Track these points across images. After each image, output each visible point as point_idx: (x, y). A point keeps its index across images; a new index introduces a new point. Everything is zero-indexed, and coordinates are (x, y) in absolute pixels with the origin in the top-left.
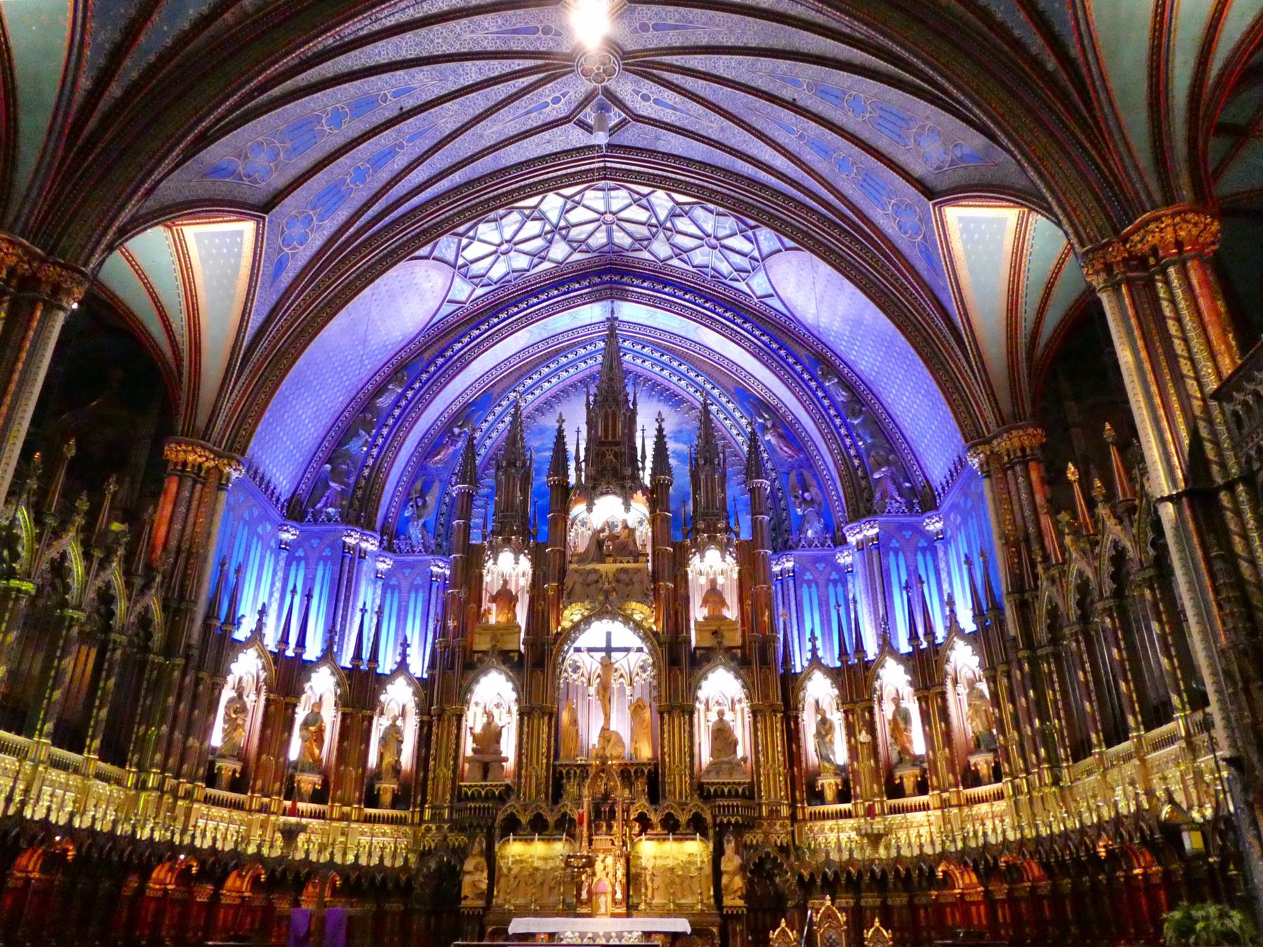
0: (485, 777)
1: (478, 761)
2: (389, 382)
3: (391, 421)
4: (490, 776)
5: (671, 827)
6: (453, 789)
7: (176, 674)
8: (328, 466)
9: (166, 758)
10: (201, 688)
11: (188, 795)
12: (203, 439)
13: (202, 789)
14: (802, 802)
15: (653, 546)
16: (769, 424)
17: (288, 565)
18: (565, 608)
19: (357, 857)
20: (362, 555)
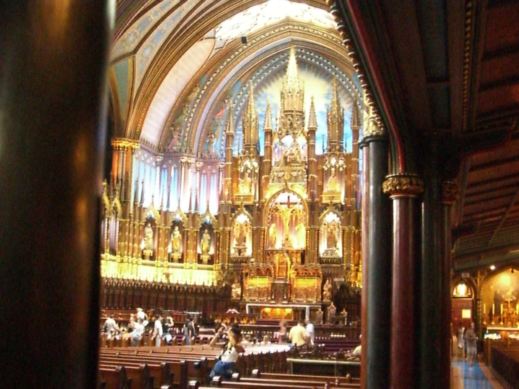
0: (240, 254)
1: (238, 249)
3: (196, 106)
4: (242, 254)
7: (127, 225)
8: (172, 128)
9: (128, 252)
10: (136, 227)
11: (137, 263)
12: (124, 137)
13: (141, 261)
15: (308, 158)
17: (161, 171)
20: (188, 164)
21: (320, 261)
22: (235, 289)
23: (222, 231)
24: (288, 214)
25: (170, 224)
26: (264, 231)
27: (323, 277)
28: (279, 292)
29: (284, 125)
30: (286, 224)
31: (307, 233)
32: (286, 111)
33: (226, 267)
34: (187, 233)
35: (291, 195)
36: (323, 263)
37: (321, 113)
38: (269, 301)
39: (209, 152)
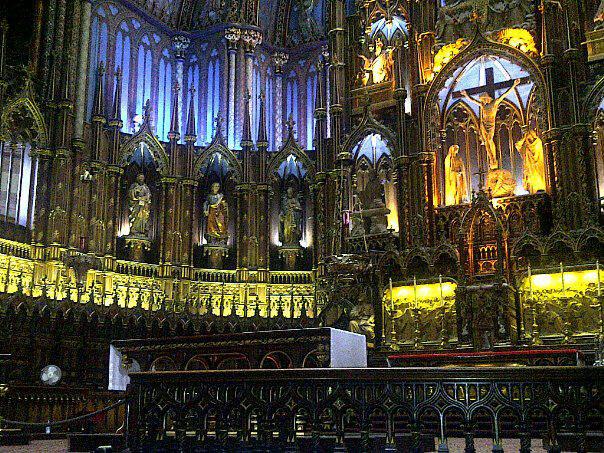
4: (373, 229)
17: (185, 72)
18: (436, 52)
19: (257, 311)
22: (356, 318)
23: (323, 180)
26: (429, 162)
28: (482, 317)
31: (550, 146)
39: (299, 29)
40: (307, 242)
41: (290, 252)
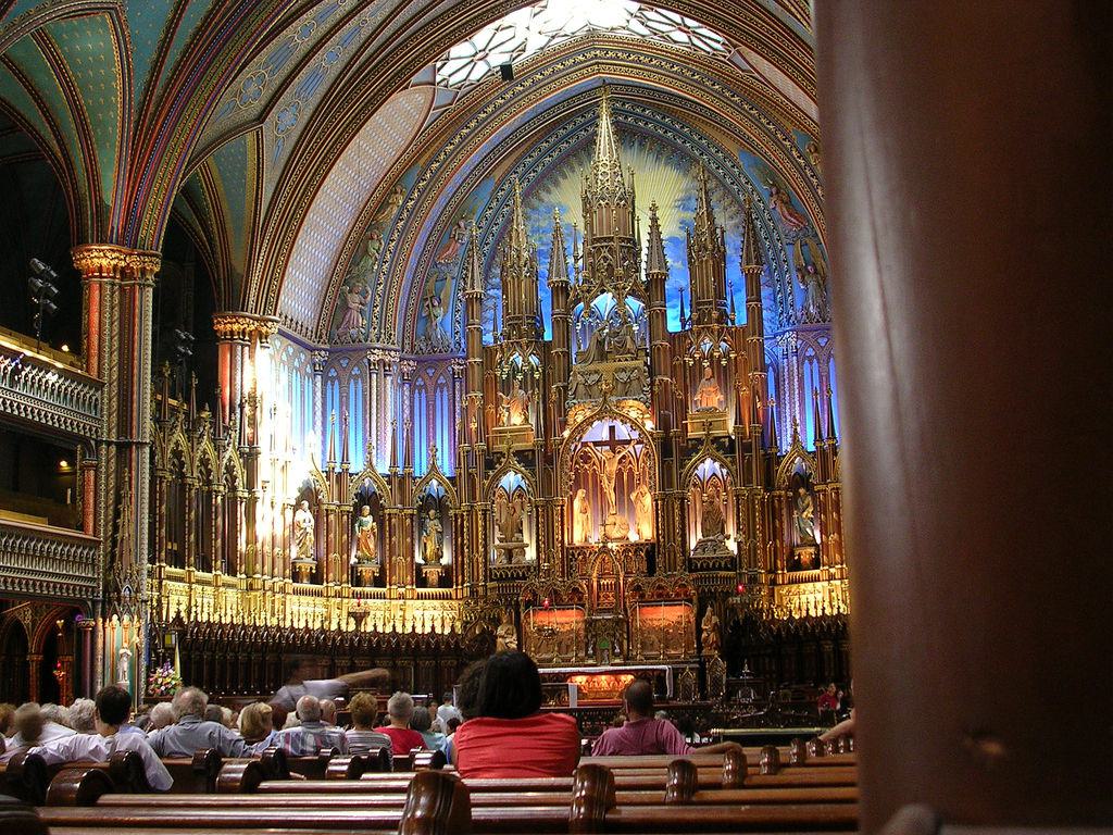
0: (510, 561)
2: (389, 195)
5: (662, 598)
6: (485, 571)
12: (242, 310)
13: (291, 585)
14: (783, 570)
16: (774, 190)
17: (324, 384)
21: (691, 565)
22: (503, 637)
24: (613, 467)
25: (352, 500)
27: (699, 599)
29: (594, 269)
30: (609, 489)
32: (598, 240)
33: (481, 590)
34: (390, 520)
35: (618, 423)
36: (696, 570)
37: (672, 239)
38: (582, 660)
40: (446, 559)
41: (432, 573)
